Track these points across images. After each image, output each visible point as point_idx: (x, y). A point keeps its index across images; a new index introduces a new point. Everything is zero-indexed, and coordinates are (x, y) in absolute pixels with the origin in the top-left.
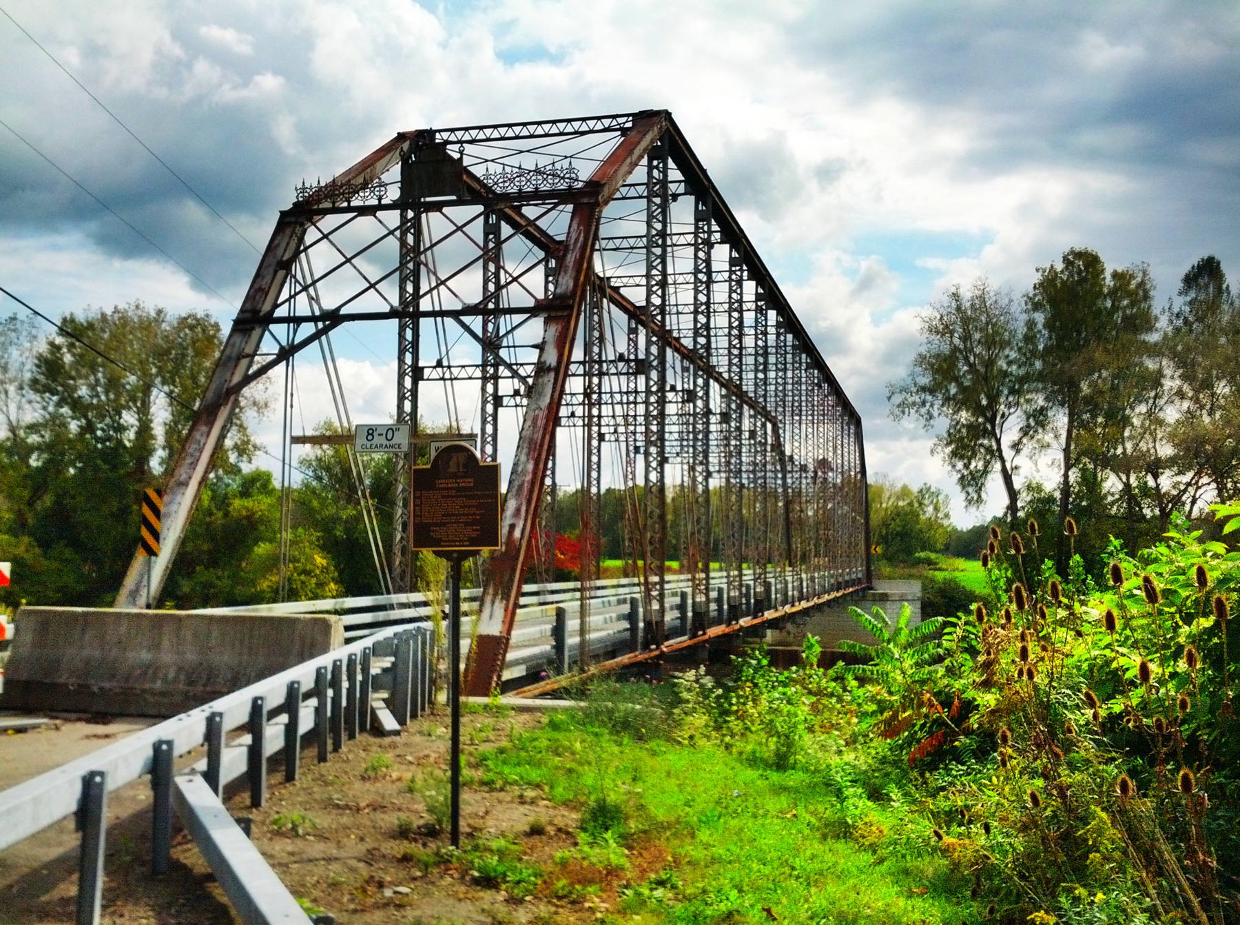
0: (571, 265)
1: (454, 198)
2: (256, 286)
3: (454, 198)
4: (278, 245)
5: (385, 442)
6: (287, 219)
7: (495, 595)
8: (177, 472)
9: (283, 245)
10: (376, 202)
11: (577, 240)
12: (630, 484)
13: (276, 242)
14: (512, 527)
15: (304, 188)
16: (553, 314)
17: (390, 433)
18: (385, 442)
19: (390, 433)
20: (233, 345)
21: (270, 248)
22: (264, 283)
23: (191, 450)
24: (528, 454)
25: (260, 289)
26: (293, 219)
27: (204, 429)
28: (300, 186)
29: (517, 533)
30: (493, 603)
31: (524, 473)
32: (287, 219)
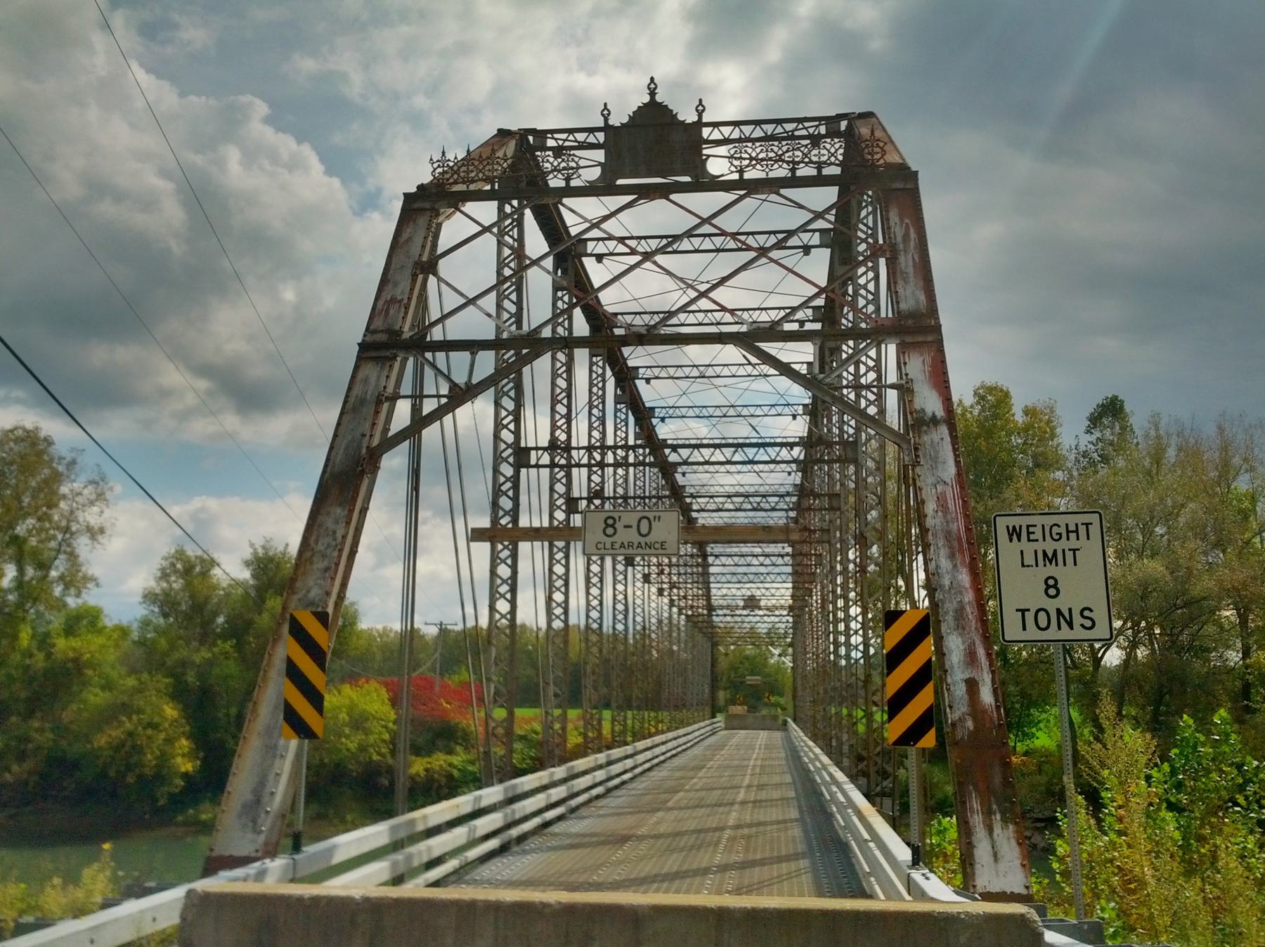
0: (911, 270)
1: (687, 179)
2: (387, 295)
3: (687, 179)
4: (409, 239)
5: (636, 539)
6: (416, 205)
7: (988, 813)
8: (299, 584)
9: (418, 240)
10: (562, 184)
11: (906, 237)
12: (558, 624)
13: (405, 236)
14: (972, 685)
15: (443, 160)
16: (909, 339)
17: (645, 523)
18: (636, 539)
19: (645, 523)
20: (366, 381)
21: (396, 244)
22: (401, 290)
23: (320, 547)
24: (952, 556)
25: (393, 300)
26: (427, 205)
27: (339, 512)
28: (437, 157)
29: (986, 696)
30: (990, 830)
31: (955, 588)
32: (416, 205)
